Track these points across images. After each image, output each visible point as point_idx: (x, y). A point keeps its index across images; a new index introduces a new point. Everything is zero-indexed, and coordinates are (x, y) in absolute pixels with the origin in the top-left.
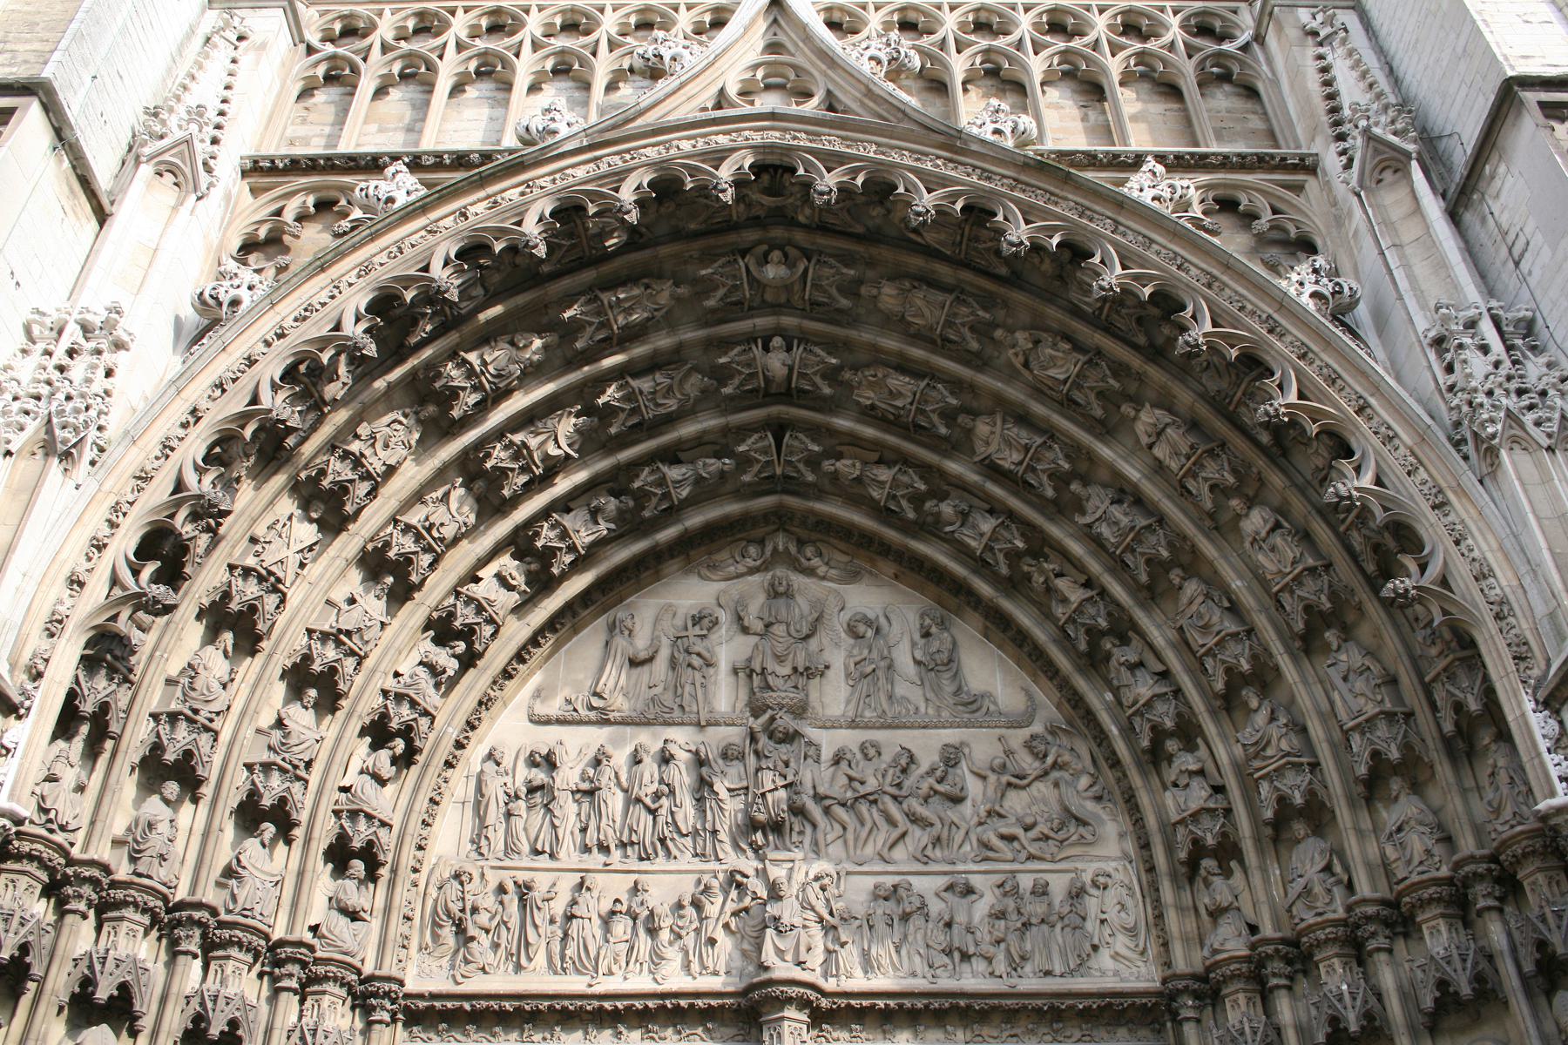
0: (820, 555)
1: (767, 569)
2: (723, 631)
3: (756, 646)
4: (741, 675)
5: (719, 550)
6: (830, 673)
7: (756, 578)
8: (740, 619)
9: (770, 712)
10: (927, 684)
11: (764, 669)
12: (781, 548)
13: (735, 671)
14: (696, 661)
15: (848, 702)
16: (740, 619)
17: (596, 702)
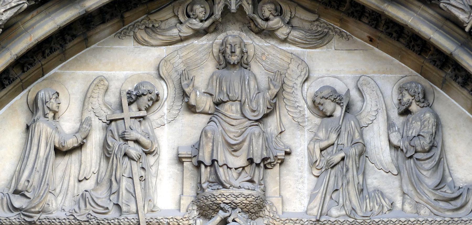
0: (280, 13)
1: (216, 30)
2: (165, 109)
3: (204, 132)
4: (187, 164)
5: (159, 10)
6: (292, 161)
7: (204, 41)
8: (185, 95)
9: (221, 214)
10: (405, 175)
11: (213, 161)
12: (233, 8)
13: (180, 160)
14: (134, 150)
15: (312, 197)
16: (185, 95)
17: (18, 202)
